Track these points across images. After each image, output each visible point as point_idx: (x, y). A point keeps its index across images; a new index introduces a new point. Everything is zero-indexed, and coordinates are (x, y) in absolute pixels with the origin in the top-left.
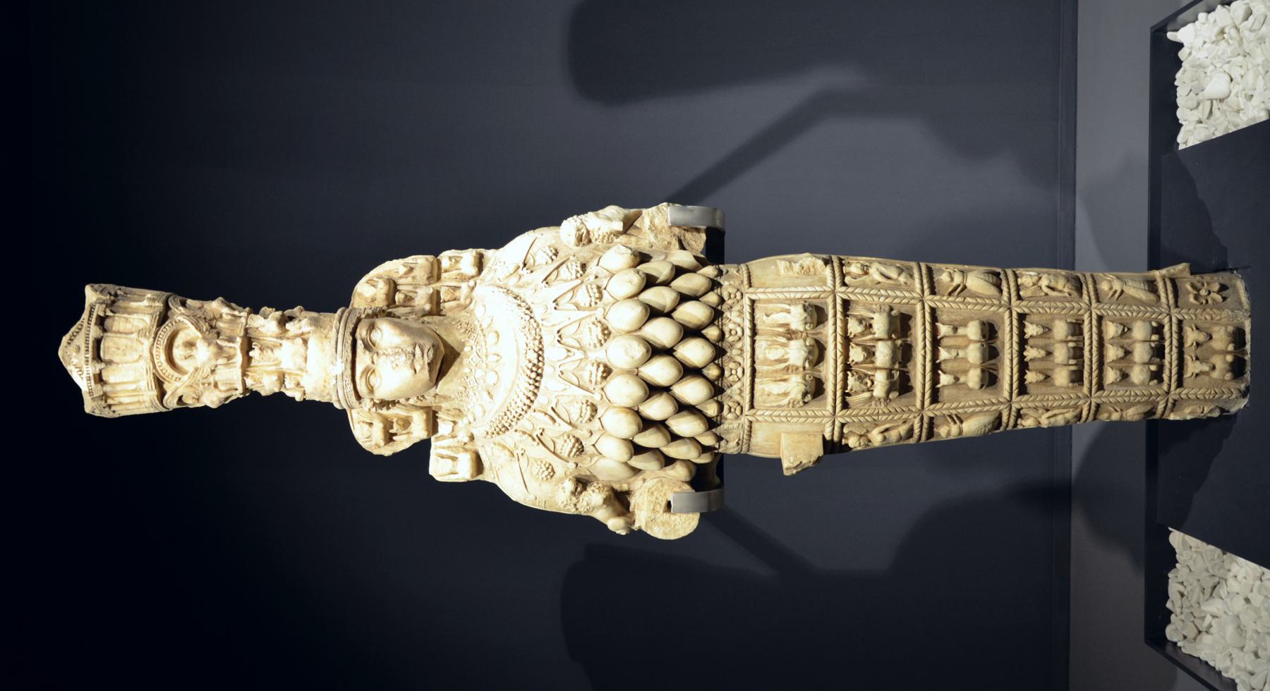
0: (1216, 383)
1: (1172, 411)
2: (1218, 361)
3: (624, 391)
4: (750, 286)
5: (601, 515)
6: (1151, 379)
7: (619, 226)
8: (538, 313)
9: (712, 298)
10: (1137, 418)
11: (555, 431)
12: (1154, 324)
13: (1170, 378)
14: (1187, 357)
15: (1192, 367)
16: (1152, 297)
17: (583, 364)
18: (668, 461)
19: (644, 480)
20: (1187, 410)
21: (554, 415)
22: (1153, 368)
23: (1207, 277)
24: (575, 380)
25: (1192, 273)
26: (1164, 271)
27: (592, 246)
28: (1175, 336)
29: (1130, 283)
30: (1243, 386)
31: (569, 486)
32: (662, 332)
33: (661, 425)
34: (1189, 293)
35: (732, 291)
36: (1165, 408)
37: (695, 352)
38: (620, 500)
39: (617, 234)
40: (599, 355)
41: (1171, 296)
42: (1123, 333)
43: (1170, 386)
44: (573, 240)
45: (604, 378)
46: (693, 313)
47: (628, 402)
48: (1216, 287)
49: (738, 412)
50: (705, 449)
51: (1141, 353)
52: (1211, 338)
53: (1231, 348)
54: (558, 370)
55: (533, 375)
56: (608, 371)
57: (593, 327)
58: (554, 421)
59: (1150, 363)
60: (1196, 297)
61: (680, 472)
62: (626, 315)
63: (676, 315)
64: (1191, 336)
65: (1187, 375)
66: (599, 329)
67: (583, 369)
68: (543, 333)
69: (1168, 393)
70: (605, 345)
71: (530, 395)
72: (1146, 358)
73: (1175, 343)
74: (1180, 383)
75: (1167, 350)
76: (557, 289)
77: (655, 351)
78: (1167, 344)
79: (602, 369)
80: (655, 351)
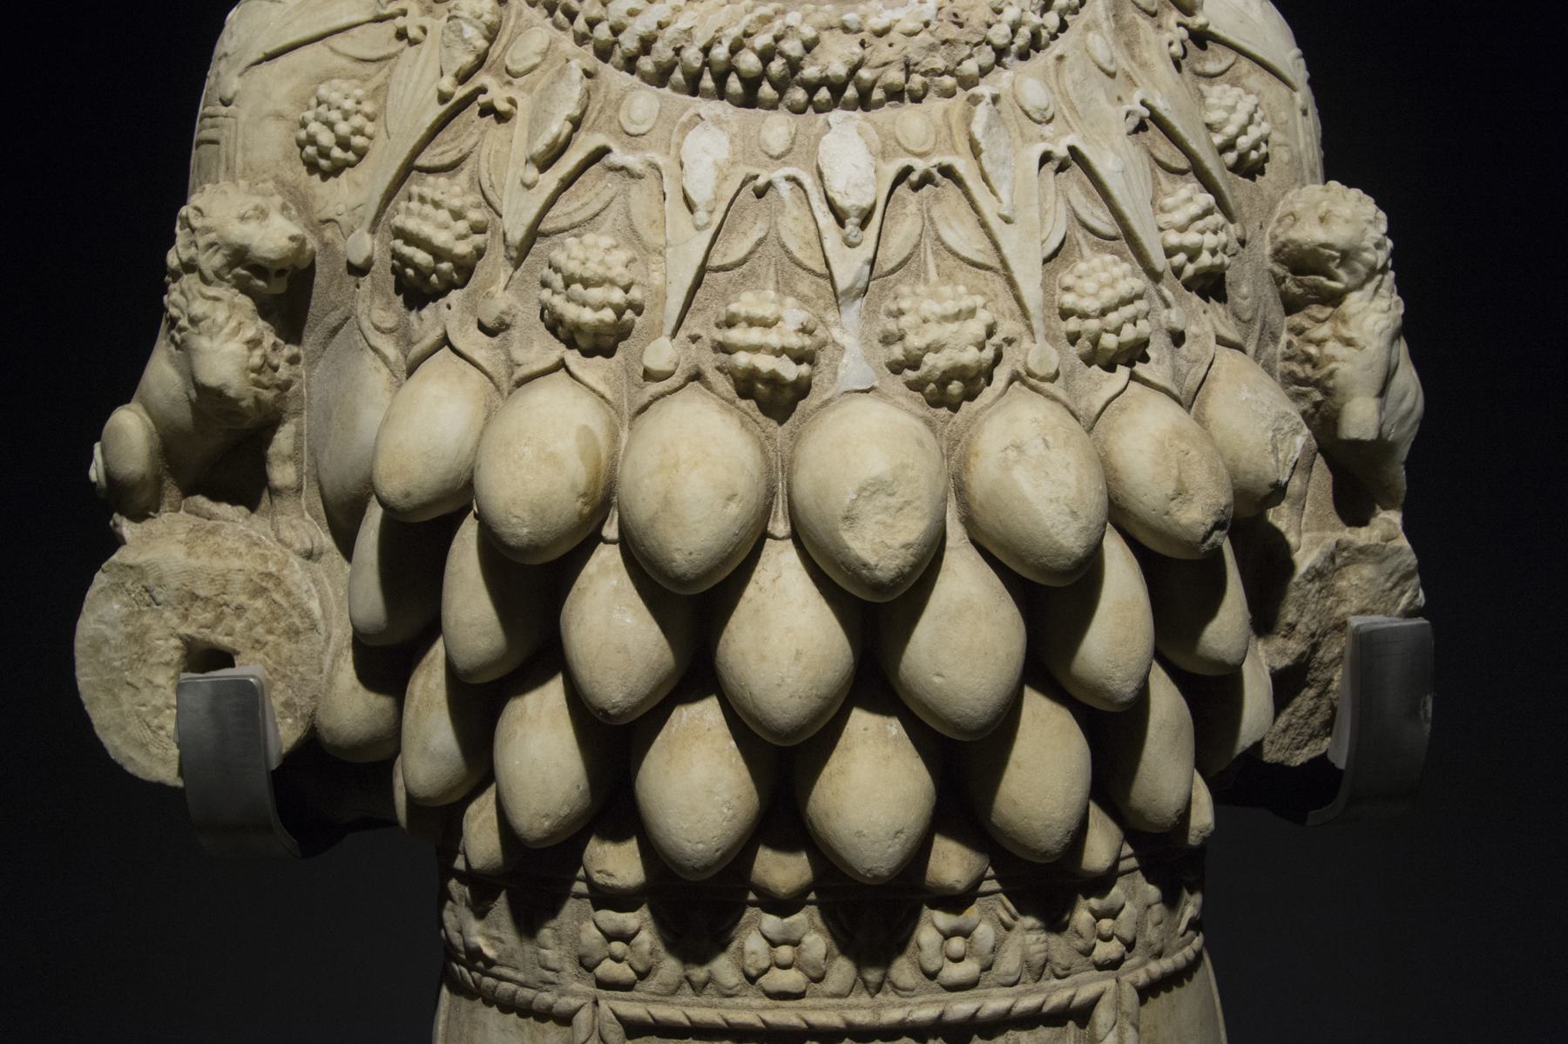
3: (695, 470)
4: (1147, 992)
5: (161, 372)
7: (1361, 418)
8: (1025, 83)
9: (1101, 846)
11: (503, 155)
17: (805, 285)
18: (385, 661)
19: (309, 555)
21: (570, 161)
24: (734, 248)
27: (1275, 313)
31: (273, 236)
32: (965, 639)
33: (538, 650)
35: (1125, 924)
37: (873, 787)
38: (226, 455)
39: (1323, 421)
40: (853, 354)
44: (1310, 233)
45: (747, 385)
46: (1045, 770)
47: (644, 489)
49: (608, 969)
50: (441, 818)
54: (778, 174)
55: (749, 61)
56: (775, 399)
57: (976, 328)
58: (545, 162)
61: (352, 707)
62: (1036, 468)
63: (1036, 706)
66: (970, 356)
67: (785, 287)
68: (934, 104)
70: (896, 384)
71: (663, 52)
76: (1117, 159)
77: (877, 613)
79: (790, 371)
80: (877, 613)
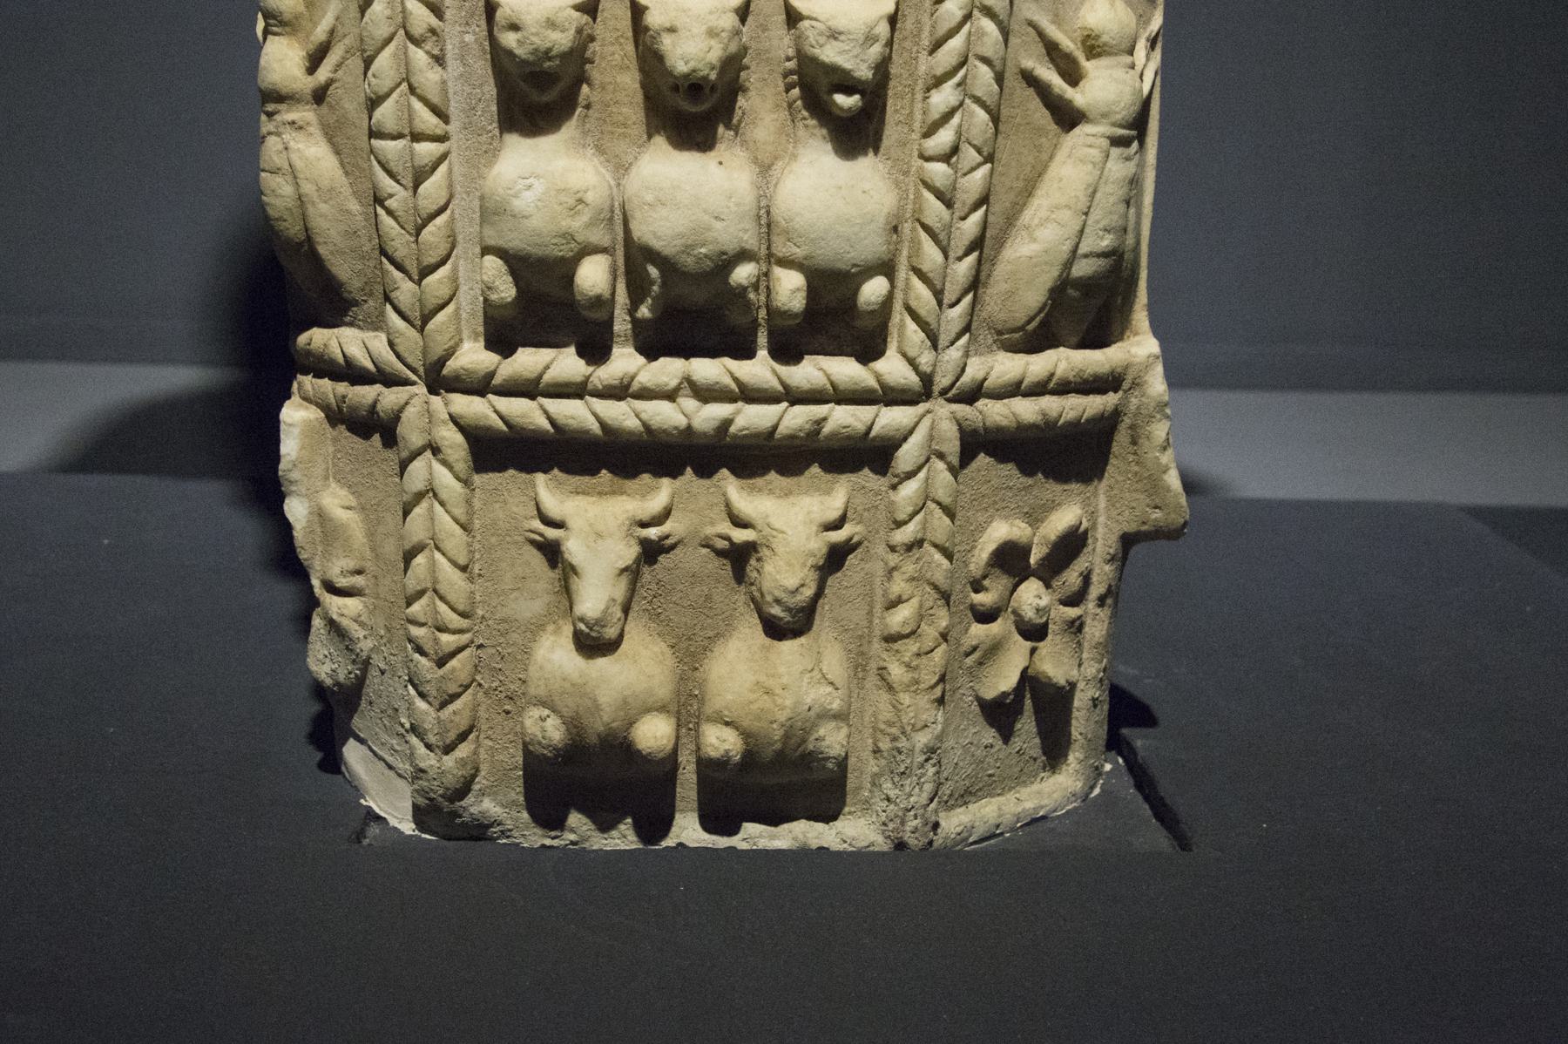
0: (502, 651)
1: (336, 416)
2: (640, 667)
6: (517, 263)
10: (278, 193)
12: (873, 290)
13: (529, 389)
14: (661, 493)
15: (598, 522)
16: (1032, 298)
20: (337, 502)
22: (593, 276)
23: (1097, 627)
25: (1128, 541)
26: (1157, 385)
28: (796, 418)
29: (1118, 168)
30: (484, 805)
34: (1034, 517)
36: (351, 373)
41: (1027, 410)
42: (814, 86)
43: (481, 386)
48: (1055, 664)
51: (689, 195)
52: (776, 630)
53: (721, 741)
59: (637, 260)
60: (1011, 560)
64: (791, 519)
65: (550, 491)
69: (439, 380)
72: (660, 228)
73: (752, 417)
74: (496, 451)
75: (707, 369)
78: (759, 369)
